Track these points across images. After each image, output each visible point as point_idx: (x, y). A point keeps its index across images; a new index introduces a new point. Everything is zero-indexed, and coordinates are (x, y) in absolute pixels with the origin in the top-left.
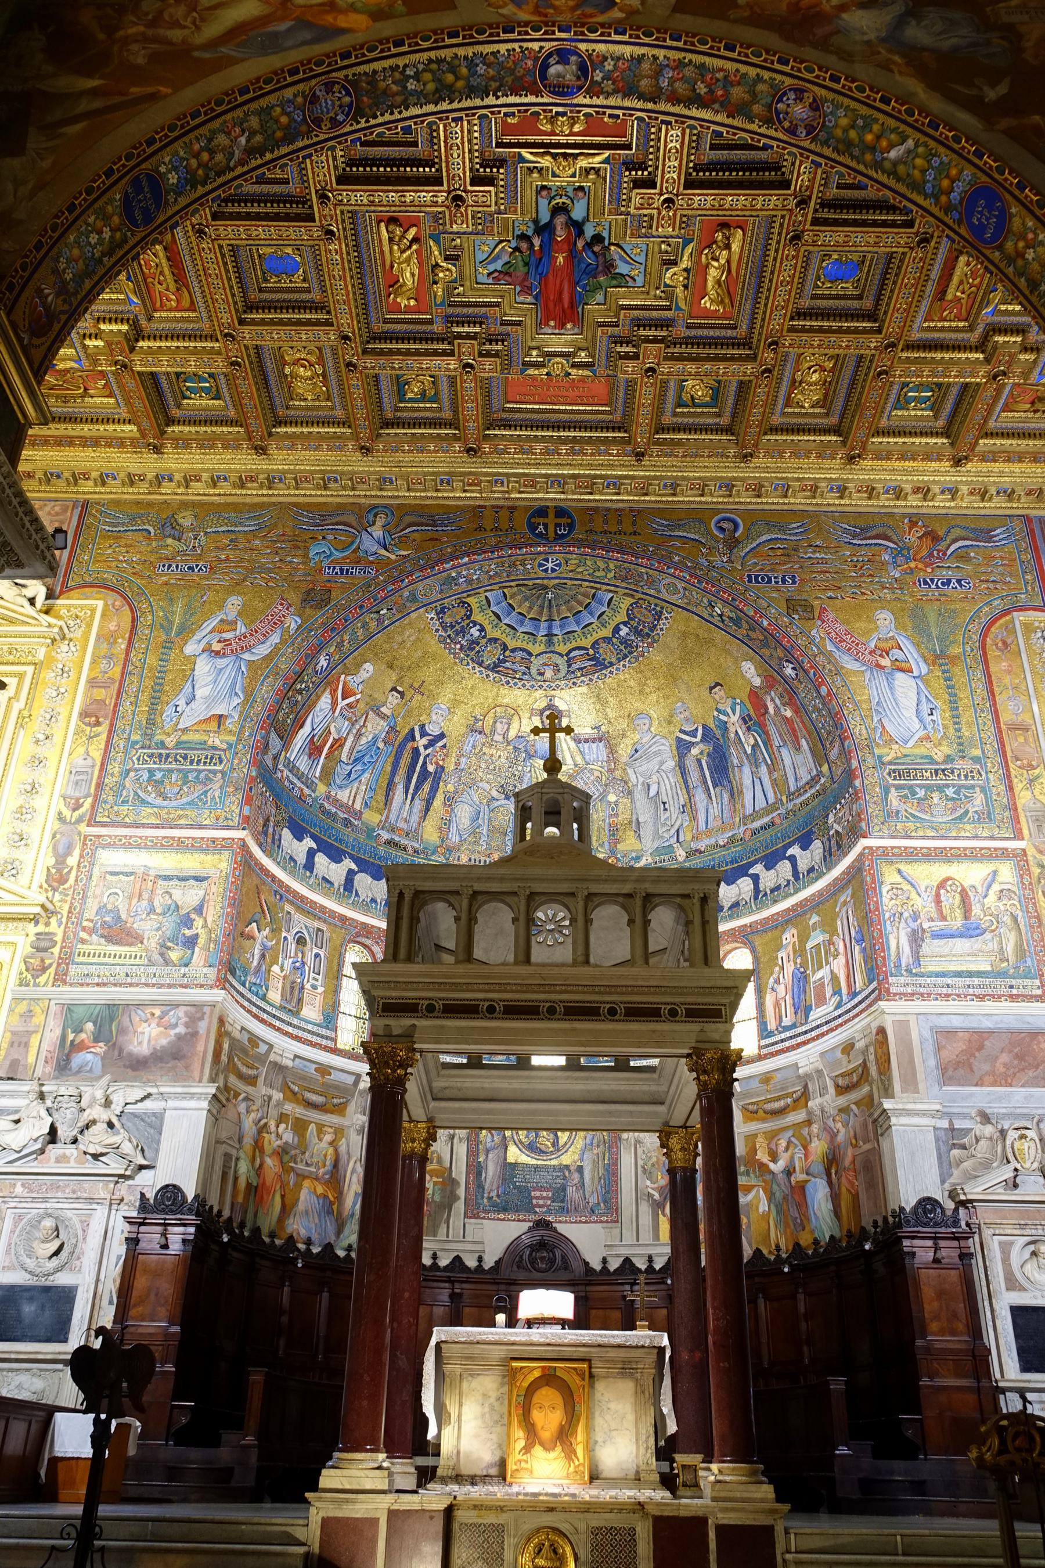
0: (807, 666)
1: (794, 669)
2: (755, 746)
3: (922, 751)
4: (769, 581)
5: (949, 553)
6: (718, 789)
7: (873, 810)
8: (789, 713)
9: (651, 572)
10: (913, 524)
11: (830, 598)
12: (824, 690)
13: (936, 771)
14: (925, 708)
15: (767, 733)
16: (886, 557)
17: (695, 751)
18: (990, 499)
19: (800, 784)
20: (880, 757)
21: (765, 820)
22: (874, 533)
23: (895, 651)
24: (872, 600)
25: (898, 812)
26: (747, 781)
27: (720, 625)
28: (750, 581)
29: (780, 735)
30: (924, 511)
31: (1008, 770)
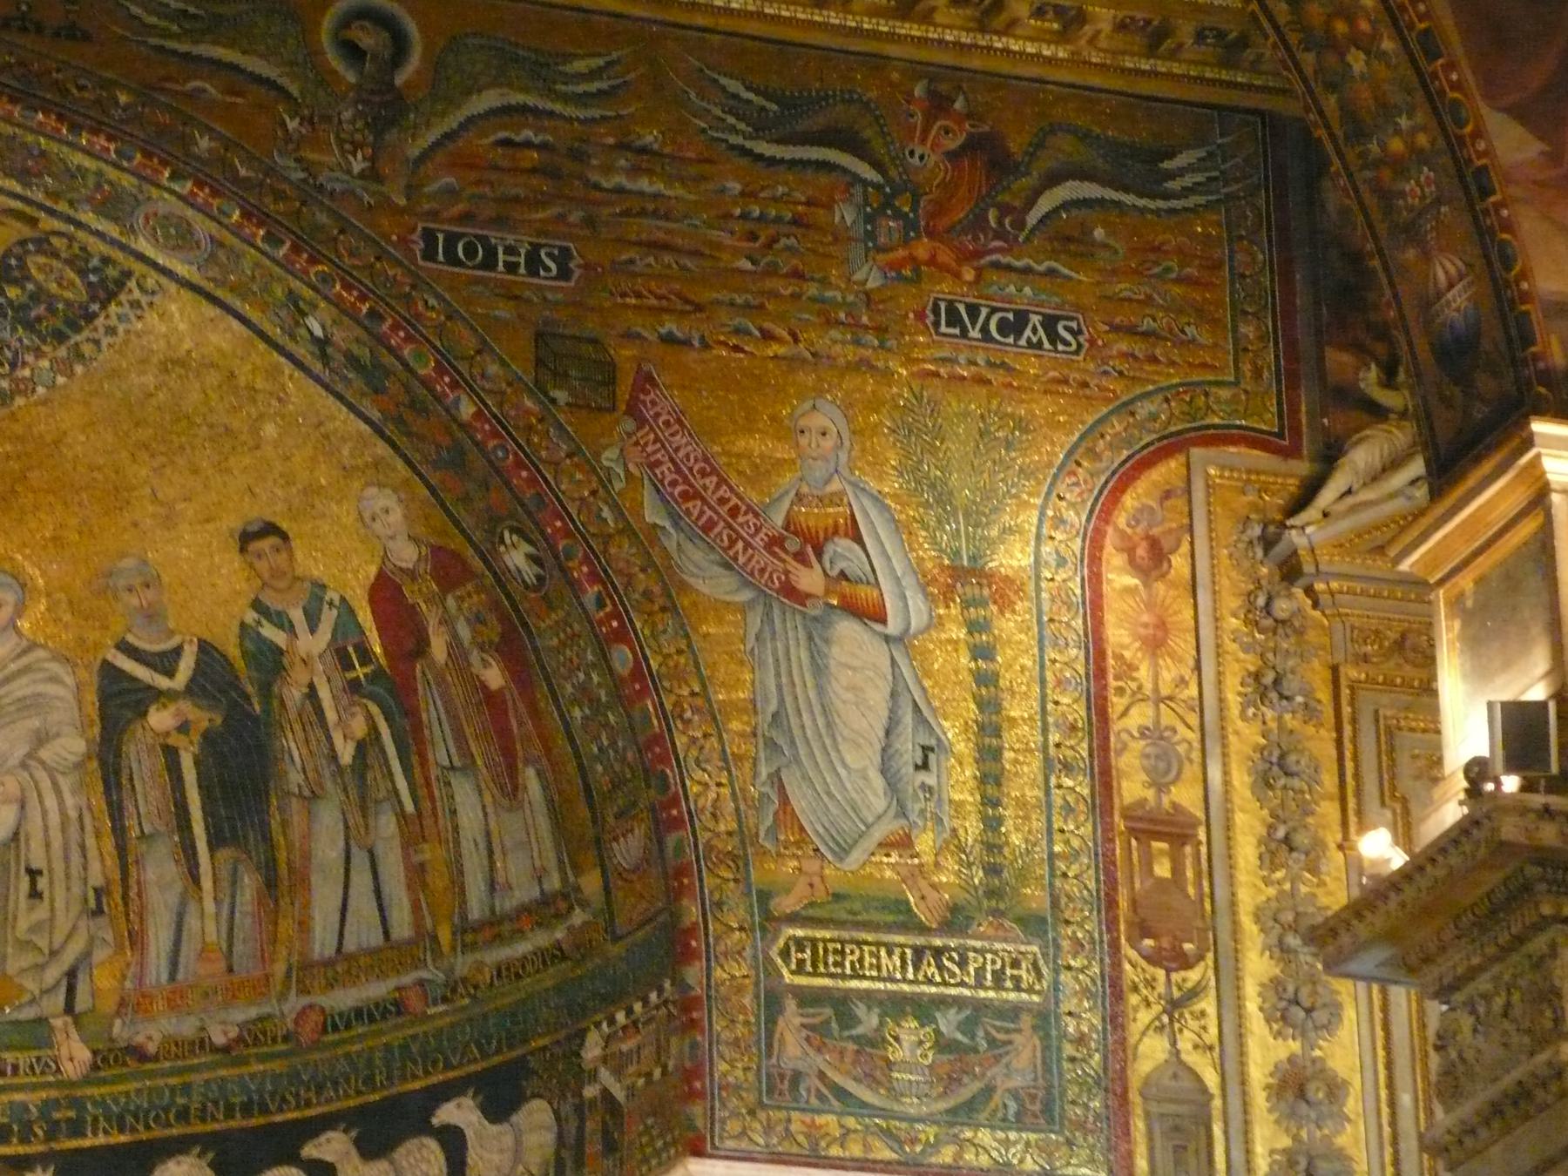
0: (580, 571)
1: (529, 557)
4: (489, 263)
5: (1032, 218)
6: (225, 854)
7: (728, 1068)
8: (494, 677)
9: (112, 174)
10: (938, 104)
11: (668, 339)
12: (622, 657)
13: (919, 952)
14: (907, 748)
15: (412, 713)
16: (846, 214)
17: (160, 719)
18: (1173, 55)
19: (507, 904)
21: (376, 990)
22: (817, 122)
23: (842, 545)
24: (793, 362)
25: (797, 1077)
26: (328, 849)
27: (317, 367)
28: (430, 254)
30: (976, 63)
31: (1117, 965)
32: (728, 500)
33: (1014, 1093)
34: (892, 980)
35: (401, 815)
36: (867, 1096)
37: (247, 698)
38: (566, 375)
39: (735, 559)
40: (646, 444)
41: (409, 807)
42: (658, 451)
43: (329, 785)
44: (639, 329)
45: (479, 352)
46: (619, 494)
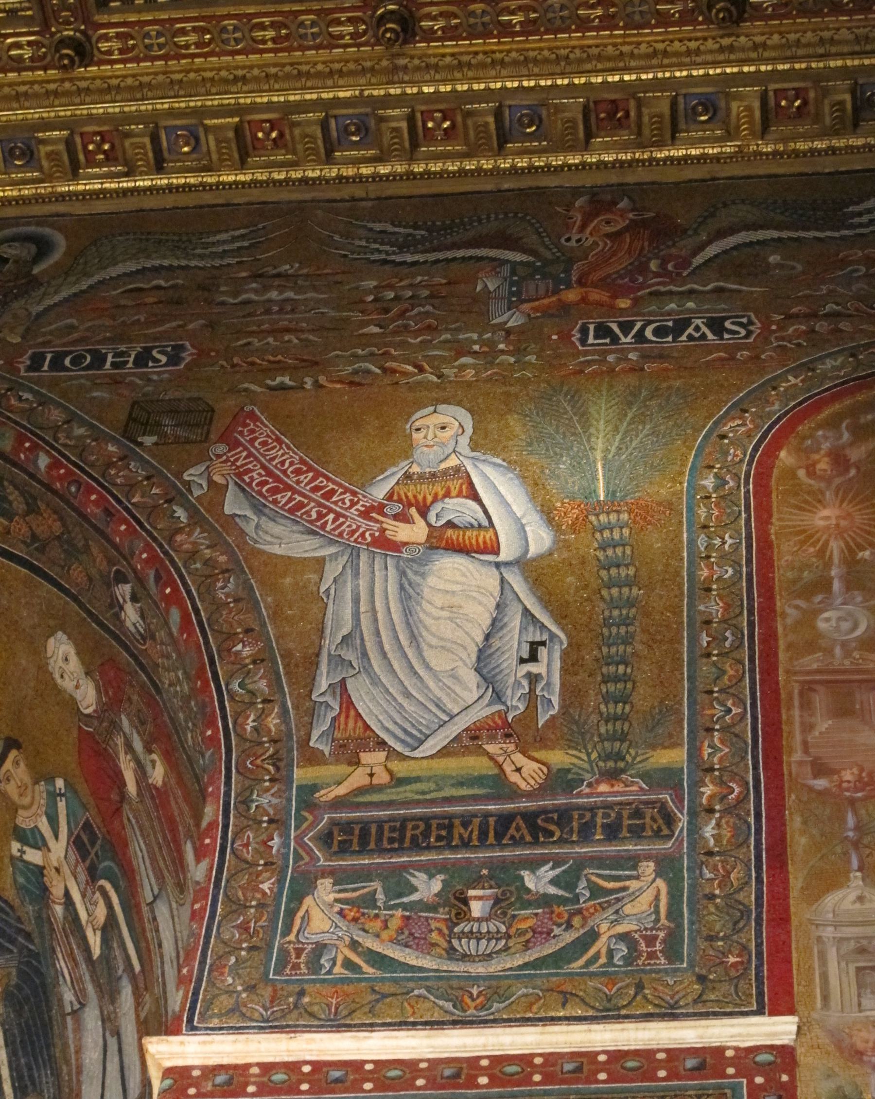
2: (109, 928)
3: (476, 765)
13: (505, 820)
20: (309, 790)
29: (153, 859)
32: (322, 488)
33: (624, 937)
34: (466, 844)
35: (133, 978)
36: (410, 957)
37: (28, 936)
38: (158, 424)
39: (323, 527)
40: (237, 460)
41: (137, 968)
42: (250, 462)
43: (90, 988)
44: (246, 385)
45: (68, 422)
46: (198, 498)
